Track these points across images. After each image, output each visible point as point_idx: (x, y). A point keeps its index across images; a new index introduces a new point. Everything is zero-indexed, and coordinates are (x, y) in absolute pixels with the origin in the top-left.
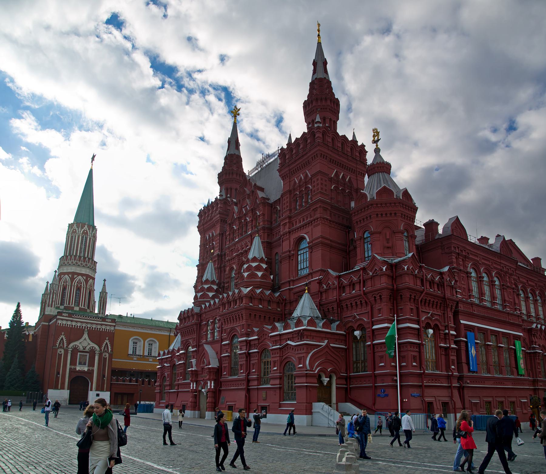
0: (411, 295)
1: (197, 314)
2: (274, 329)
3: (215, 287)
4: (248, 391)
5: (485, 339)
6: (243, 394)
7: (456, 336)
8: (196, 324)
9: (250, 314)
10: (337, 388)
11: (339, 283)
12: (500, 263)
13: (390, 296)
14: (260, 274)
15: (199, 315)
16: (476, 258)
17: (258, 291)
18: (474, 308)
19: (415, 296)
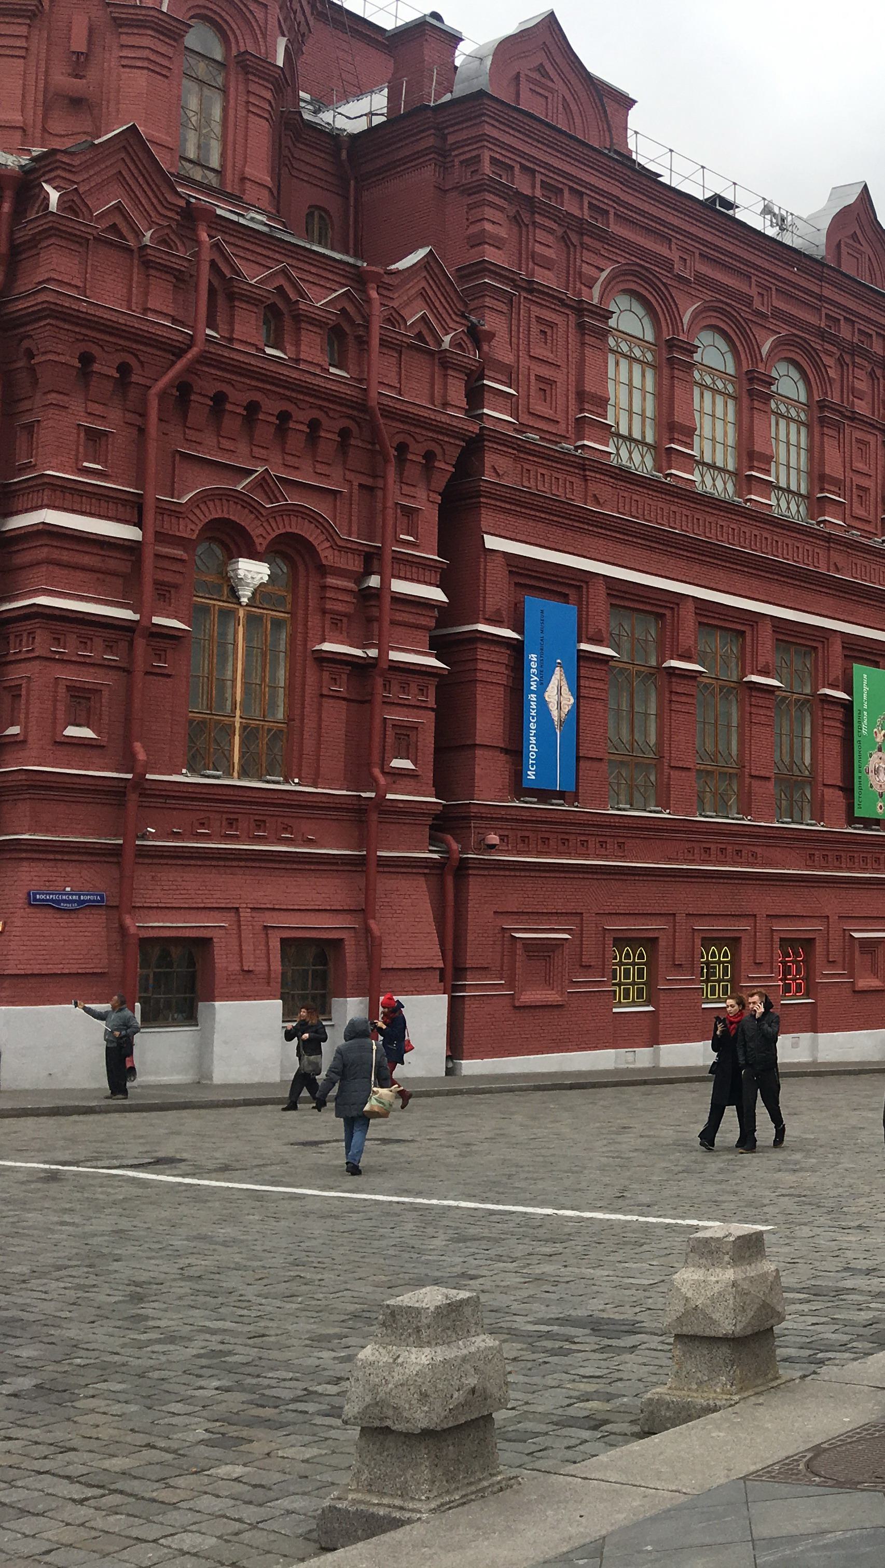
0: (87, 359)
7: (445, 614)
12: (821, 298)
16: (663, 250)
18: (603, 489)
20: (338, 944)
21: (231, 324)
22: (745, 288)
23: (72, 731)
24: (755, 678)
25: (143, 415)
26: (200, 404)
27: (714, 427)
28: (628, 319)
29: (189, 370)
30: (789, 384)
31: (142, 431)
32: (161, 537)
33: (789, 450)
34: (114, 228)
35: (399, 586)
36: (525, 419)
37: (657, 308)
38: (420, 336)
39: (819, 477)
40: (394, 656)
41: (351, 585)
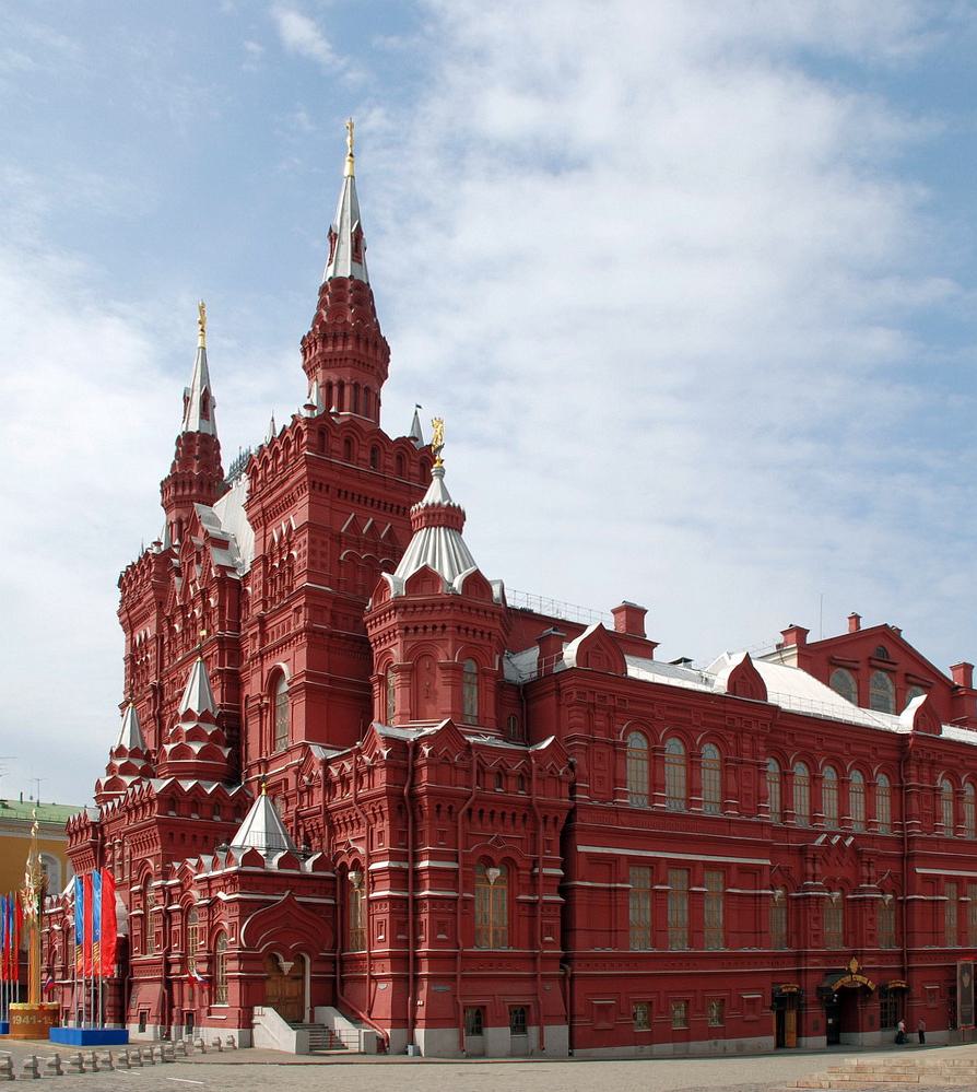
1: (93, 824)
2: (199, 866)
3: (139, 764)
4: (168, 984)
5: (652, 879)
6: (158, 987)
7: (563, 879)
8: (93, 845)
9: (171, 834)
10: (312, 979)
11: (340, 773)
12: (725, 712)
13: (400, 807)
14: (196, 748)
15: (98, 828)
17: (188, 785)
19: (450, 808)
20: (528, 1007)
21: (484, 782)
22: (688, 717)
23: (439, 937)
24: (694, 889)
25: (457, 822)
26: (475, 814)
27: (675, 776)
28: (637, 742)
29: (473, 804)
30: (710, 753)
31: (457, 827)
32: (464, 865)
33: (711, 781)
34: (445, 757)
35: (546, 871)
36: (595, 795)
37: (651, 736)
38: (551, 772)
39: (725, 794)
40: (545, 898)
41: (528, 873)
